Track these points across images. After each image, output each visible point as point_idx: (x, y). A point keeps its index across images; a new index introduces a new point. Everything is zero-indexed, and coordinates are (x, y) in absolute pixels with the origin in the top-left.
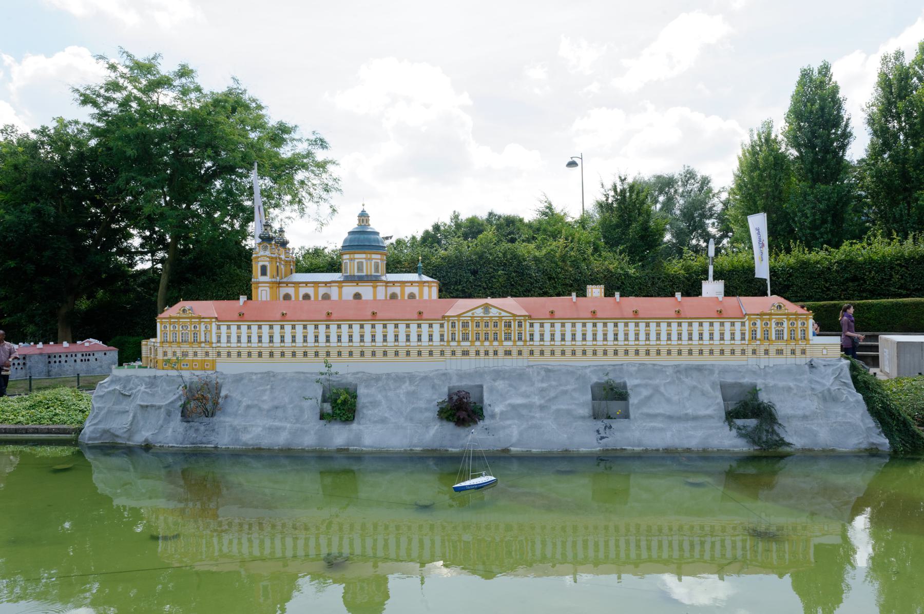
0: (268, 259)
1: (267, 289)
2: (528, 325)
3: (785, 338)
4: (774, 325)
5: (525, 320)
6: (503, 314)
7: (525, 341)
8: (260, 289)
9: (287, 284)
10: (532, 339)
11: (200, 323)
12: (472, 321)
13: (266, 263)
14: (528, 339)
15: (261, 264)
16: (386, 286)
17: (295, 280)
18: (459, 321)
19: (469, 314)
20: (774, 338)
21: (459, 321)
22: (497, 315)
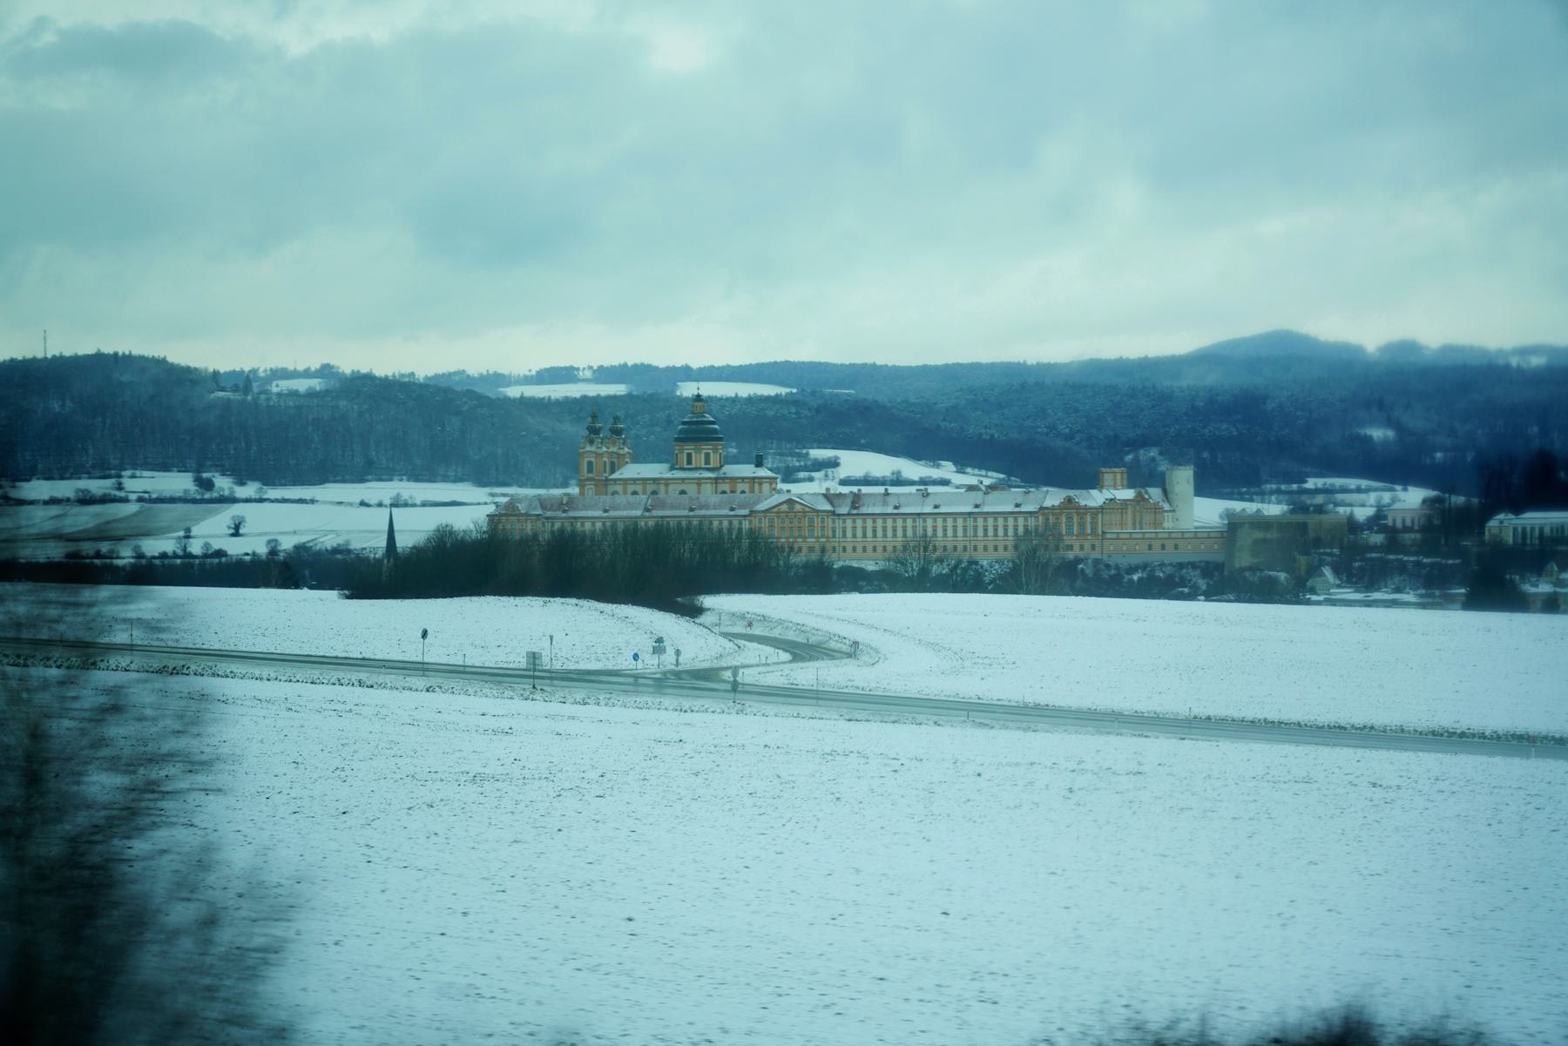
0: (594, 455)
1: (593, 487)
2: (830, 521)
3: (1075, 532)
4: (1064, 520)
5: (828, 516)
6: (807, 509)
7: (828, 537)
8: (586, 487)
9: (615, 480)
10: (834, 536)
11: (526, 520)
12: (778, 517)
13: (593, 460)
14: (831, 535)
15: (587, 460)
16: (716, 483)
17: (625, 476)
18: (765, 517)
19: (776, 510)
20: (1064, 533)
21: (765, 517)
22: (801, 510)
